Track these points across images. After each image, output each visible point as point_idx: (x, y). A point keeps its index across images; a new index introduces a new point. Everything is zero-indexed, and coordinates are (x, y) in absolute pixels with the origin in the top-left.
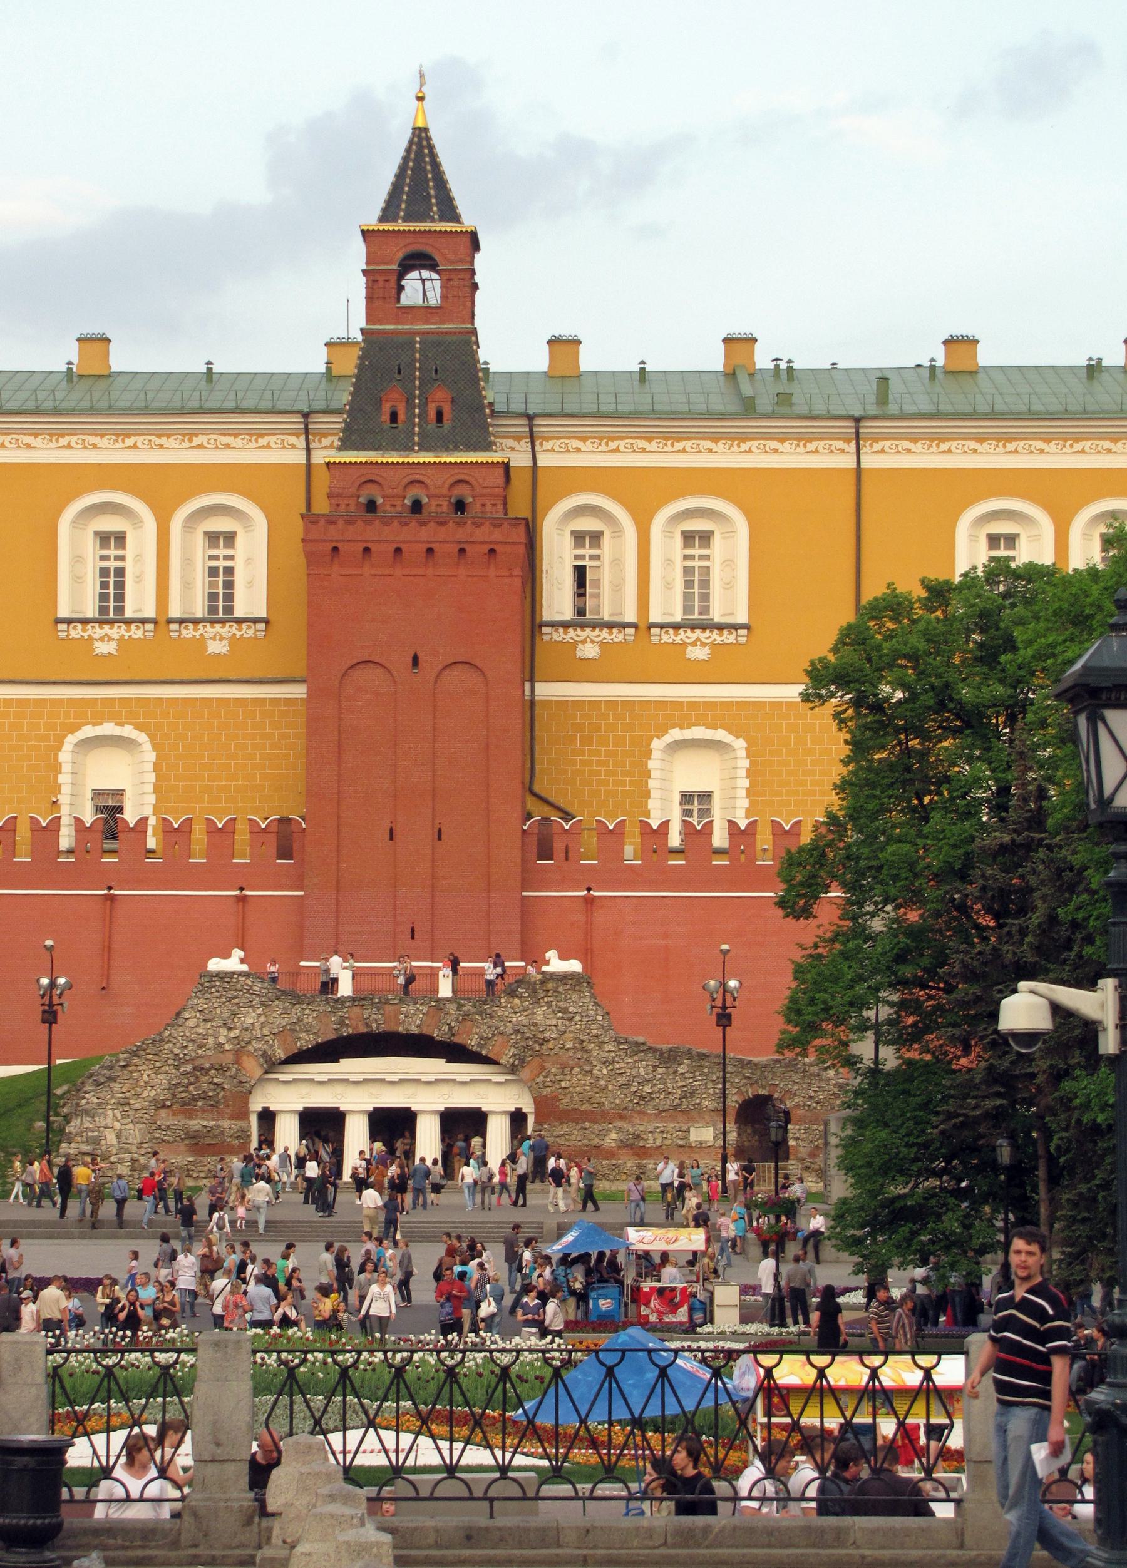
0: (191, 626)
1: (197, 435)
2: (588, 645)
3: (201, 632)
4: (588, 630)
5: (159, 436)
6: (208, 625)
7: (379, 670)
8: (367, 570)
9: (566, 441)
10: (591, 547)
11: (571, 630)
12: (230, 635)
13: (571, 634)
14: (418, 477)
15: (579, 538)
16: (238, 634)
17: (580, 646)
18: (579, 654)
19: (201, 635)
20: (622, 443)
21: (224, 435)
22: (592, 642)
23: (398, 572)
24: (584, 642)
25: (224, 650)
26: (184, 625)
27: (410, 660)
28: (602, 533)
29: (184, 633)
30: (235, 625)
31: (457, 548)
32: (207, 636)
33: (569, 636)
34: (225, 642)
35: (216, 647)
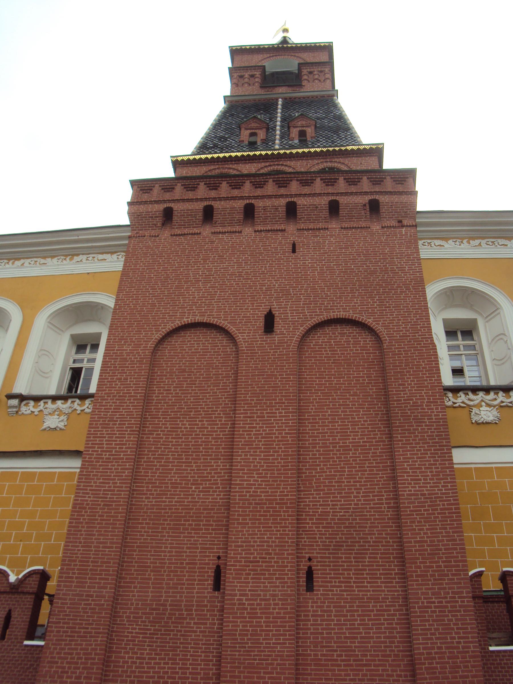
0: (32, 403)
1: (78, 255)
2: (484, 408)
3: (41, 408)
4: (481, 394)
5: (45, 258)
6: (50, 401)
7: (212, 334)
8: (207, 231)
9: (429, 241)
10: (463, 340)
11: (461, 394)
12: (70, 411)
13: (462, 397)
14: (279, 168)
15: (450, 334)
16: (79, 408)
17: (475, 410)
18: (475, 419)
19: (41, 411)
20: (483, 242)
21: (102, 253)
22: (488, 405)
23: (248, 230)
24: (479, 406)
25: (61, 425)
26: (24, 402)
27: (261, 323)
28: (474, 322)
29: (24, 409)
30: (78, 401)
31: (324, 201)
32: (46, 412)
33: (459, 400)
34: (62, 418)
35: (52, 422)
